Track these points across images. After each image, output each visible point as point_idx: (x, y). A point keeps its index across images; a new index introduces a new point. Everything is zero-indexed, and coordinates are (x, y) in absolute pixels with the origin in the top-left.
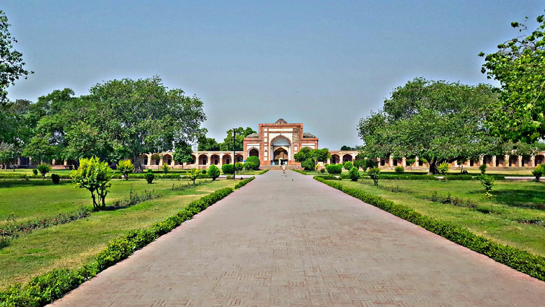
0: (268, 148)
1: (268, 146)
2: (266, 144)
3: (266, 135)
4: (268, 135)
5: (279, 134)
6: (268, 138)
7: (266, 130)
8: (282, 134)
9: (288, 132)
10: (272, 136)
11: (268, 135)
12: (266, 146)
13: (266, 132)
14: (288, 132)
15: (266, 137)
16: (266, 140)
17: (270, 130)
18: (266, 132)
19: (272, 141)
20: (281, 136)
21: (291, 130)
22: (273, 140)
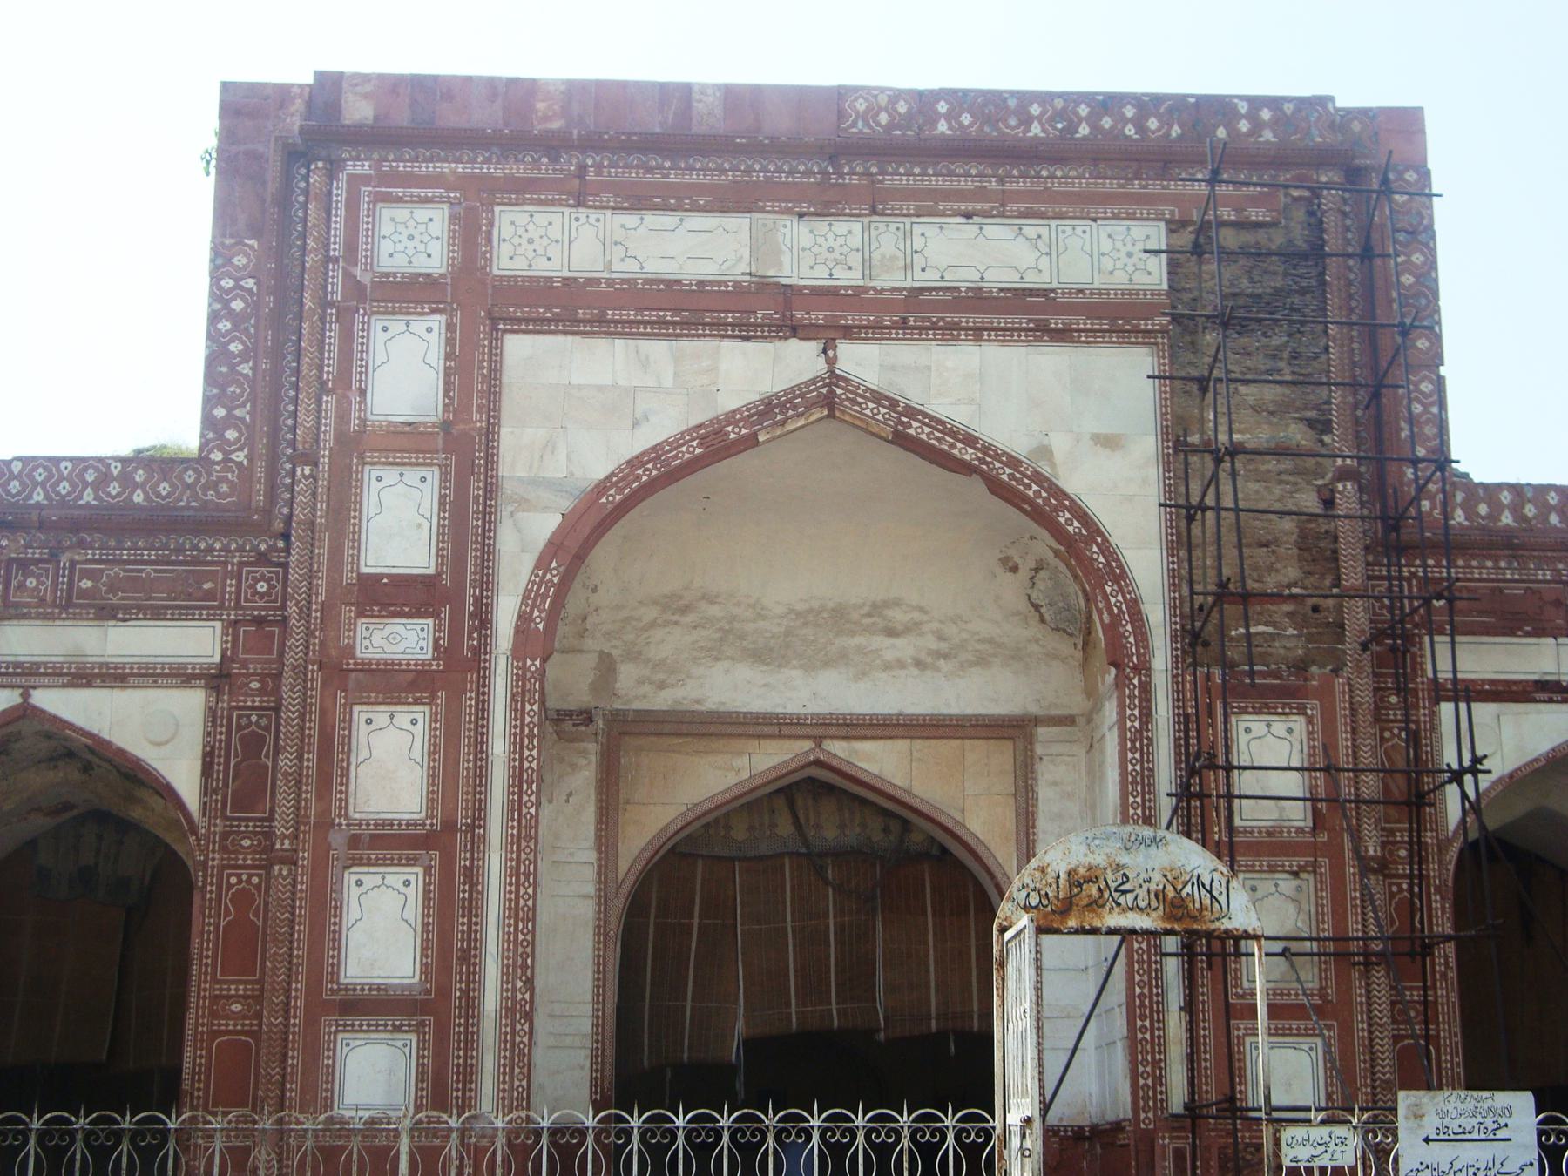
0: (456, 760)
1: (449, 681)
2: (405, 640)
3: (404, 370)
4: (474, 382)
5: (798, 362)
6: (463, 448)
7: (413, 237)
8: (863, 361)
9: (1039, 316)
10: (583, 412)
11: (474, 382)
12: (394, 683)
13: (409, 294)
14: (1039, 316)
15: (405, 443)
16: (398, 525)
17: (541, 240)
18: (409, 294)
19: (572, 550)
20: (829, 397)
21: (1120, 253)
22: (598, 518)
